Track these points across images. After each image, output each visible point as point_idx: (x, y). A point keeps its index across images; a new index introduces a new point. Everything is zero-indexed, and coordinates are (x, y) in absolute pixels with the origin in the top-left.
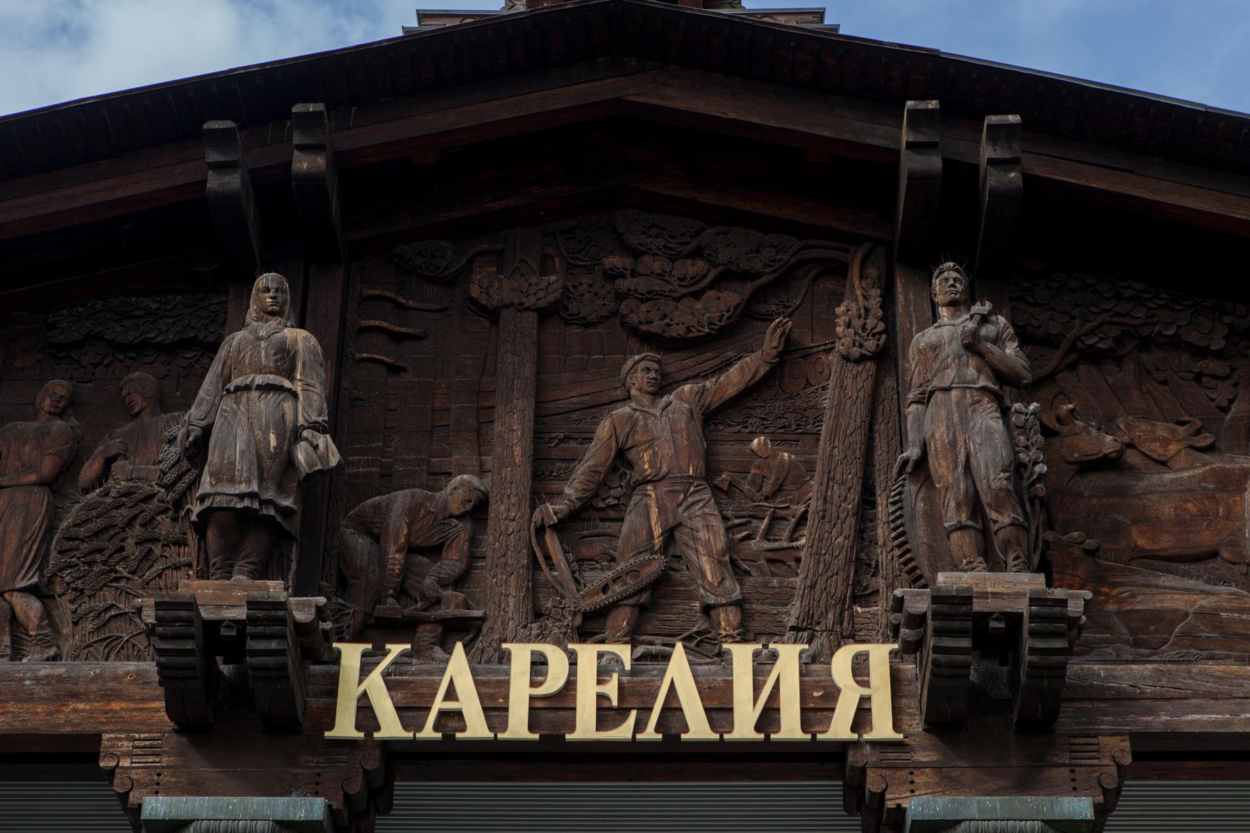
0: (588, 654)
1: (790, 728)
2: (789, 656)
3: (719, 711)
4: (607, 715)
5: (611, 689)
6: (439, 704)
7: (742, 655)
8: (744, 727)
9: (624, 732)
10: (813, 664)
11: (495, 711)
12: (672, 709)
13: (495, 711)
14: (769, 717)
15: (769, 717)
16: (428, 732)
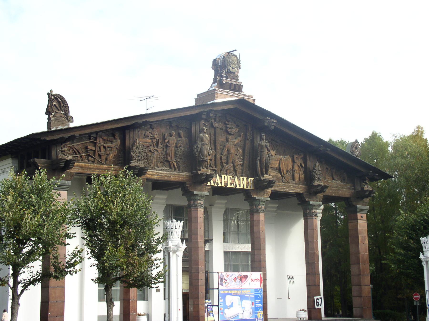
0: (229, 176)
1: (245, 188)
2: (245, 178)
3: (240, 185)
4: (231, 184)
5: (231, 181)
6: (216, 182)
7: (241, 178)
8: (242, 187)
9: (232, 186)
10: (247, 179)
11: (221, 183)
12: (236, 184)
13: (221, 183)
14: (244, 186)
15: (244, 186)
16: (216, 185)
